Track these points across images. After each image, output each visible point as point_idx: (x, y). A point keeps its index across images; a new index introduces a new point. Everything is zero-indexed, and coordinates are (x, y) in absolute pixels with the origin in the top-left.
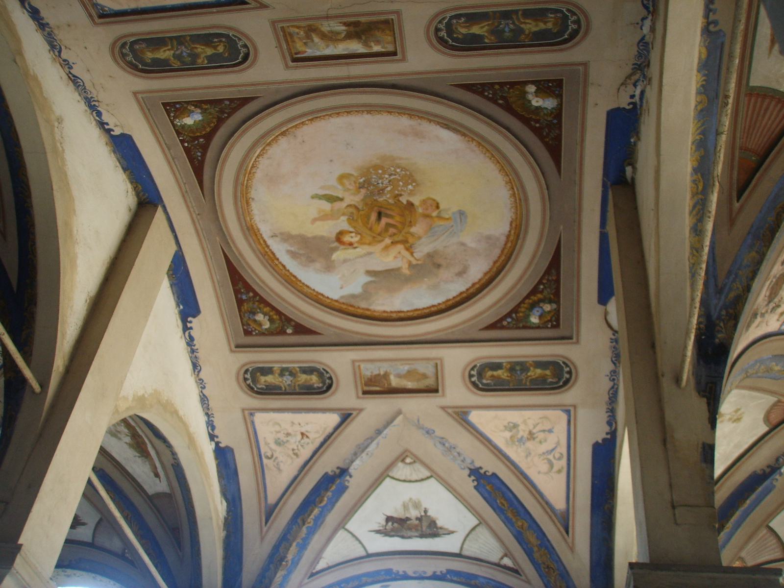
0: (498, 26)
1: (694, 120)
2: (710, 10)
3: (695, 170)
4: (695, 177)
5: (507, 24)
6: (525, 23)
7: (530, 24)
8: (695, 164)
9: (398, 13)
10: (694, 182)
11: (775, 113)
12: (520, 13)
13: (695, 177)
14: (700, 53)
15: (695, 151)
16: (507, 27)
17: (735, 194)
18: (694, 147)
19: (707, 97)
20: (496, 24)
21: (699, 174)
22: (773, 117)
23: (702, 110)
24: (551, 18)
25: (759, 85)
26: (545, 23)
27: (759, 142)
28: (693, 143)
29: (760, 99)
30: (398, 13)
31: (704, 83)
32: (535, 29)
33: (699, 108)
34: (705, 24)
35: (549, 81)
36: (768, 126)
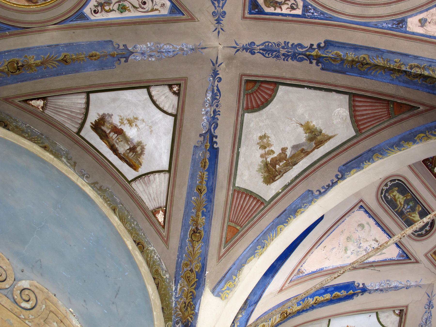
0: (409, 212)
1: (388, 156)
2: (333, 183)
3: (414, 142)
4: (418, 141)
5: (406, 209)
6: (400, 203)
7: (399, 201)
8: (411, 143)
9: (426, 255)
10: (421, 140)
11: (362, 109)
12: (396, 210)
13: (418, 141)
14: (354, 173)
15: (404, 147)
16: (407, 209)
17: (416, 111)
18: (402, 149)
19: (373, 155)
20: (408, 213)
21: (415, 139)
22: (364, 108)
23: (381, 154)
24: (390, 196)
25: (353, 129)
26: (394, 196)
27: (382, 107)
28: (400, 150)
29: (360, 123)
30: (426, 255)
31: (367, 161)
32: (401, 196)
33: (381, 156)
34: (340, 180)
35: (427, 166)
36: (370, 108)
